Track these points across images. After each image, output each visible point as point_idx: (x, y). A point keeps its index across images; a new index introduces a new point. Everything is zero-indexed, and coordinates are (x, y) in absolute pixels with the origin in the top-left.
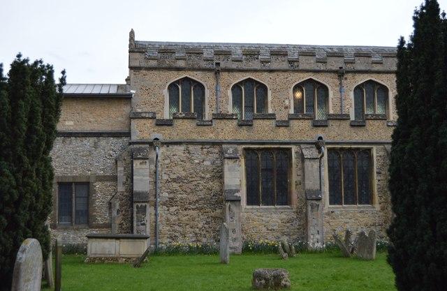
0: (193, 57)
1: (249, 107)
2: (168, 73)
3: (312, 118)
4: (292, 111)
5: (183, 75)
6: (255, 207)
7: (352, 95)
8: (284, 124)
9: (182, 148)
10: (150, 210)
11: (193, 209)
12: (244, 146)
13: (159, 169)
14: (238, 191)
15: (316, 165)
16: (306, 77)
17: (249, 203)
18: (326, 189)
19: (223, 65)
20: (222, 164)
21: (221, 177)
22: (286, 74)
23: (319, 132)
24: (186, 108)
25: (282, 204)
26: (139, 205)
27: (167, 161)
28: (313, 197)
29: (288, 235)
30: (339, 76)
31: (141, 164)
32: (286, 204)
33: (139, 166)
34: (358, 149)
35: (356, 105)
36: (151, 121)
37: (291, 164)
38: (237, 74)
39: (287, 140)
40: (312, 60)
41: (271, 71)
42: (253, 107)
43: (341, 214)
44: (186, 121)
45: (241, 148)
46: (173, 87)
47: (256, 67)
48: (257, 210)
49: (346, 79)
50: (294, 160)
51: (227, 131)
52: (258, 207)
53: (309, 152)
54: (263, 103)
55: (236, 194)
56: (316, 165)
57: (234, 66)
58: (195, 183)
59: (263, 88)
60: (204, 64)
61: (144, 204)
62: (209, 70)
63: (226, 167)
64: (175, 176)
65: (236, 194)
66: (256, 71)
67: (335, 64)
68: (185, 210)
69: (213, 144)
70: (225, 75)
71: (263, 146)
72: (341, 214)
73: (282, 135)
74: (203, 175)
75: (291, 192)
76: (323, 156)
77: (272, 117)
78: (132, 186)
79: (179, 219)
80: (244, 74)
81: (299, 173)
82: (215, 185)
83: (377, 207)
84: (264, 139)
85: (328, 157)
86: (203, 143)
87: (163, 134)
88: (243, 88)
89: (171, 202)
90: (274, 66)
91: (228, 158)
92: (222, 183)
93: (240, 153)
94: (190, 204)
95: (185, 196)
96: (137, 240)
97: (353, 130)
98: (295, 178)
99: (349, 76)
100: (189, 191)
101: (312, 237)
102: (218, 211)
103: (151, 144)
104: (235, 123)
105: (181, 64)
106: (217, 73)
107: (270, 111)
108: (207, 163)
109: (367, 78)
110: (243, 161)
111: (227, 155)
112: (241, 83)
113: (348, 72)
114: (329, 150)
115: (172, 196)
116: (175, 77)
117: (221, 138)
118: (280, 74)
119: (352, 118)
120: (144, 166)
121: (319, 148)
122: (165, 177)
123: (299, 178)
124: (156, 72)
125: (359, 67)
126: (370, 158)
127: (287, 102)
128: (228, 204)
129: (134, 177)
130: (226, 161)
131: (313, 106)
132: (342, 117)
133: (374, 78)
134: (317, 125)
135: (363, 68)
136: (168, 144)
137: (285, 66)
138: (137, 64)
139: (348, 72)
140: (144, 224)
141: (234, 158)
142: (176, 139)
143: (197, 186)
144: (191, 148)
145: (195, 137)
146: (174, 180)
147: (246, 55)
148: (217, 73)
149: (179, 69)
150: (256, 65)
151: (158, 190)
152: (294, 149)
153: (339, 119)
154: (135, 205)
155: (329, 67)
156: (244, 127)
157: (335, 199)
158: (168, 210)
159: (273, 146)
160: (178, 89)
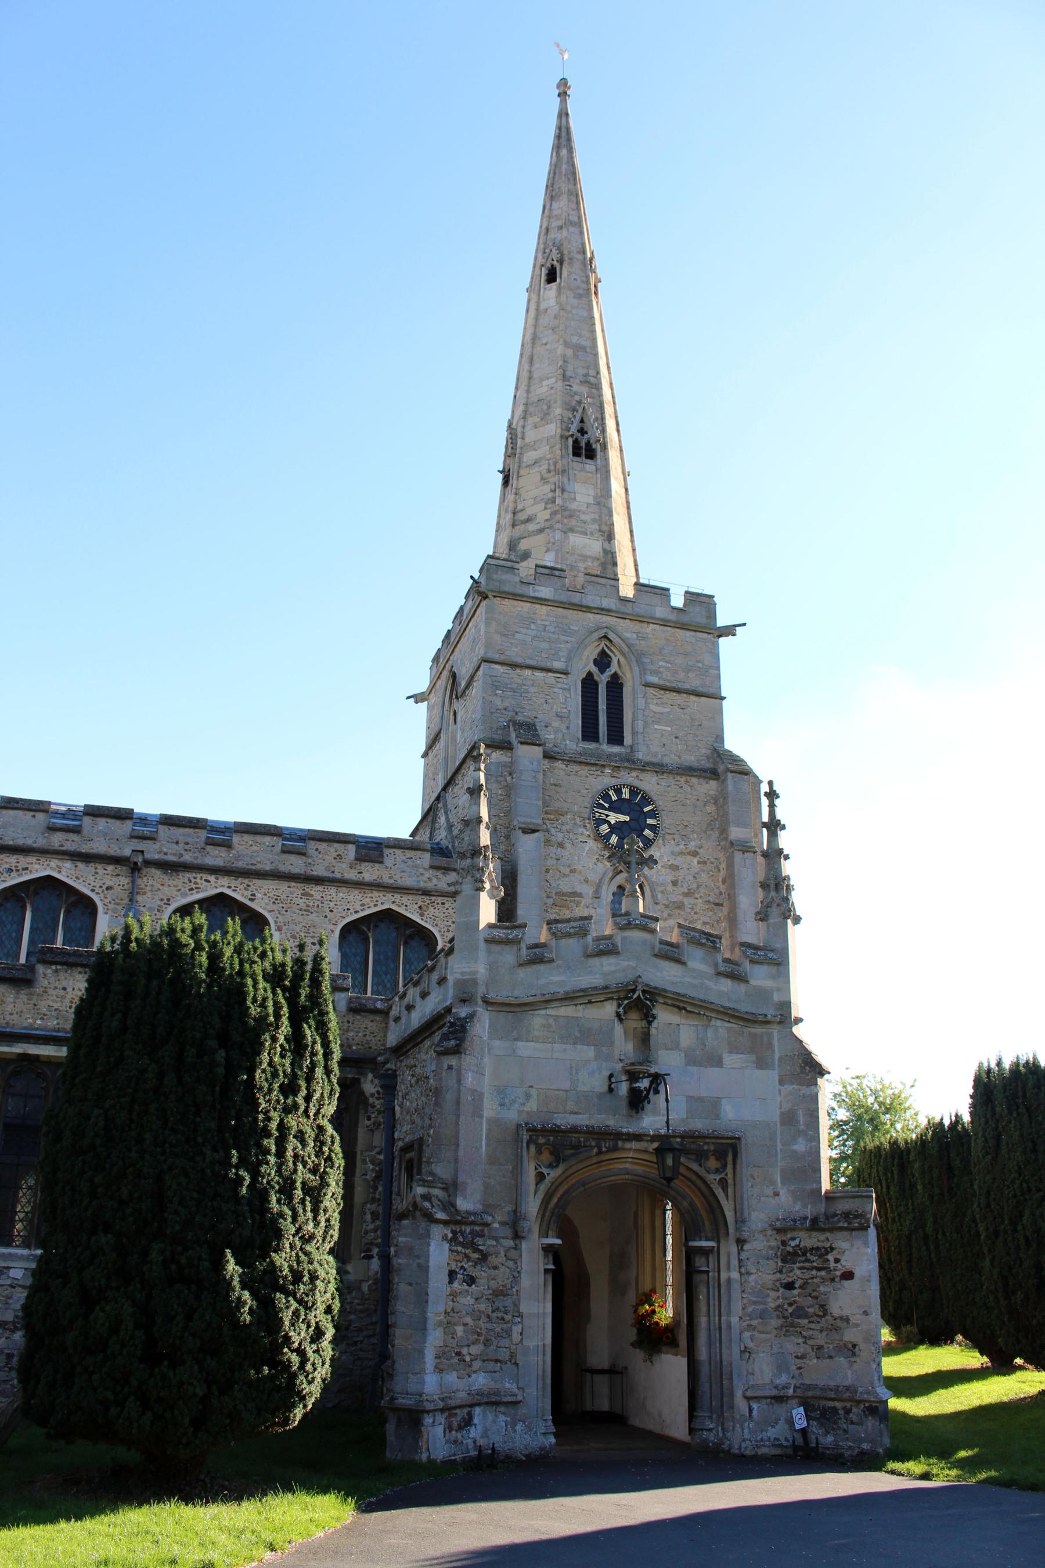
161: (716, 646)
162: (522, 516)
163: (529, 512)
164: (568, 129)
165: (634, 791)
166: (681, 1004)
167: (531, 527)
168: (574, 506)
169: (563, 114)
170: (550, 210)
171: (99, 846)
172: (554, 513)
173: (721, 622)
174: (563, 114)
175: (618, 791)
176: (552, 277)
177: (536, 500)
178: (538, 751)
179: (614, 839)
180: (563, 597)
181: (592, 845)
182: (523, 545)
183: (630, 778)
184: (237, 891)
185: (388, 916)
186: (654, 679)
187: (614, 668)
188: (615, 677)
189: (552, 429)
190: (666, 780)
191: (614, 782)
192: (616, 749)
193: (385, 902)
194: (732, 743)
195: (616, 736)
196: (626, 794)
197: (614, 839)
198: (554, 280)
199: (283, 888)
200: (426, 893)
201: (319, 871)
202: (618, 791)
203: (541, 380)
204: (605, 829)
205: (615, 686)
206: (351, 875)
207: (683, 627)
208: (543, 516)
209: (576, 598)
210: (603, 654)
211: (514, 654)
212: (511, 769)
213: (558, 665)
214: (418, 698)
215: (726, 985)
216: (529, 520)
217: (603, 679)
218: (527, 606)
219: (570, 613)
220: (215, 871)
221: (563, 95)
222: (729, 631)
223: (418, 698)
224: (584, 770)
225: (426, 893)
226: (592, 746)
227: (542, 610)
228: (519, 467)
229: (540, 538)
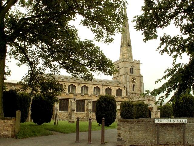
15: (74, 103)
16: (71, 84)
23: (75, 97)
28: (73, 110)
53: (73, 101)
73: (67, 97)
83: (86, 113)
84: (64, 98)
97: (82, 96)
109: (84, 85)
114: (77, 100)
121: (75, 100)
125: (82, 82)
126: (85, 102)
133: (86, 85)
137: (67, 81)
155: (76, 82)
157: (77, 111)
166: (151, 100)
171: (100, 84)
173: (140, 63)
182: (124, 54)
184: (109, 87)
185: (119, 89)
194: (141, 74)
195: (133, 73)
199: (113, 87)
205: (133, 68)
212: (126, 77)
220: (108, 86)
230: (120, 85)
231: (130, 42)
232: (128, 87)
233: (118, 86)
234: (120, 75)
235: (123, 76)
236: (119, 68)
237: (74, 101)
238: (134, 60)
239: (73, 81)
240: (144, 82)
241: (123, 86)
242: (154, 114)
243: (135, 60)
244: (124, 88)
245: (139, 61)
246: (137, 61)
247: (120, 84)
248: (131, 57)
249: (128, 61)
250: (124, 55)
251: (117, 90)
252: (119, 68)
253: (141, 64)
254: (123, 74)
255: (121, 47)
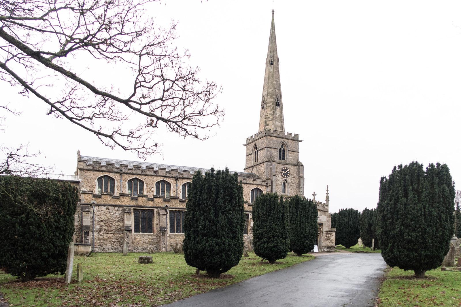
0: (110, 166)
1: (136, 190)
2: (97, 173)
3: (162, 197)
4: (155, 194)
5: (105, 174)
6: (138, 233)
7: (181, 187)
8: (152, 200)
9: (105, 207)
10: (91, 233)
11: (110, 234)
12: (134, 208)
13: (95, 216)
14: (131, 226)
15: (165, 217)
16: (162, 179)
17: (135, 231)
18: (168, 227)
19: (124, 171)
20: (124, 215)
21: (123, 220)
22: (153, 177)
24: (106, 189)
25: (150, 232)
26: (86, 231)
27: (98, 213)
29: (152, 245)
30: (176, 179)
31: (86, 213)
32: (152, 232)
33: (85, 215)
34: (182, 211)
35: (183, 192)
36: (91, 195)
37: (154, 216)
38: (130, 176)
39: (152, 206)
40: (164, 172)
41: (146, 175)
42: (137, 190)
43: (174, 237)
44: (107, 196)
45: (132, 208)
46: (100, 179)
47: (139, 173)
48: (139, 234)
49: (179, 181)
50: (155, 214)
51: (126, 201)
52: (139, 233)
53: (163, 212)
54: (142, 189)
55: (130, 228)
56: (165, 217)
57: (129, 172)
58: (111, 222)
59: (142, 182)
60: (115, 170)
61: (88, 231)
62: (118, 173)
63: (125, 216)
64: (102, 219)
65: (130, 228)
66: (139, 175)
67: (174, 174)
68: (107, 234)
69: (120, 206)
70: (125, 176)
71: (142, 208)
72: (174, 237)
73: (151, 204)
74: (115, 219)
75: (154, 228)
76: (167, 213)
77: (146, 196)
78: (82, 223)
79: (104, 238)
80: (133, 176)
81: (158, 220)
82: (121, 224)
85: (170, 214)
86: (115, 206)
87: (96, 201)
88: (133, 182)
89: (100, 230)
90: (148, 173)
91: (127, 213)
92: (124, 223)
93: (132, 210)
94: (109, 231)
95: (107, 228)
96: (86, 246)
98: (155, 221)
99: (180, 180)
100: (108, 226)
101: (162, 246)
102: (122, 235)
103: (91, 205)
104: (130, 198)
105: (104, 169)
106: (121, 174)
107: (145, 193)
108: (117, 214)
110: (133, 214)
111: (126, 211)
112: (132, 179)
113: (180, 178)
114: (170, 211)
115: (101, 227)
116: (101, 174)
117: (123, 204)
118: (150, 177)
119: (181, 198)
120: (87, 215)
121: (166, 211)
122: (98, 220)
123: (157, 222)
124: (92, 172)
127: (153, 189)
128: (126, 232)
129: (83, 219)
130: (126, 214)
131: (164, 191)
132: (176, 198)
134: (165, 201)
135: (186, 176)
136: (99, 205)
137: (152, 173)
138: (82, 167)
139: (180, 178)
140: (88, 239)
141: (130, 213)
142: (103, 203)
143: (112, 224)
144: (110, 207)
145: (112, 203)
146: (102, 221)
147: (135, 167)
148: (121, 174)
149: (103, 171)
150: (139, 172)
151: (94, 225)
152: (155, 210)
153: (175, 199)
154: (83, 232)
155: (172, 175)
156: (134, 200)
157: (172, 231)
158: (99, 234)
159: (146, 208)
160: (102, 180)
161: (298, 143)
162: (267, 117)
163: (269, 116)
164: (274, 24)
165: (287, 168)
167: (269, 119)
168: (276, 116)
169: (273, 20)
170: (271, 46)
172: (273, 118)
173: (299, 139)
174: (273, 20)
175: (284, 168)
176: (272, 64)
177: (270, 114)
178: (275, 163)
179: (284, 176)
180: (277, 136)
181: (281, 176)
182: (268, 123)
183: (286, 166)
185: (257, 188)
186: (290, 150)
187: (284, 148)
188: (284, 149)
189: (272, 100)
190: (291, 166)
191: (284, 167)
192: (284, 161)
193: (257, 186)
195: (284, 159)
196: (286, 169)
197: (284, 176)
198: (272, 65)
200: (262, 185)
201: (248, 182)
202: (284, 168)
203: (271, 88)
204: (283, 174)
205: (284, 150)
206: (252, 183)
207: (294, 140)
208: (271, 117)
209: (279, 136)
210: (282, 145)
211: (270, 146)
212: (271, 165)
213: (276, 147)
214: (244, 145)
215: (322, 208)
216: (269, 118)
217: (282, 149)
218: (272, 138)
219: (278, 138)
221: (273, 14)
222: (301, 141)
223: (244, 145)
224: (280, 165)
225: (262, 185)
226: (280, 160)
227: (274, 138)
228: (266, 107)
229: (271, 122)
230: (259, 182)
231: (281, 98)
232: (274, 184)
233: (255, 182)
234: (258, 163)
235: (265, 164)
236: (256, 149)
237: (164, 212)
238: (286, 134)
239: (165, 175)
240: (304, 176)
241: (263, 184)
242: (325, 236)
243: (289, 134)
244: (267, 187)
245: (296, 135)
246: (293, 136)
247: (258, 180)
248: (282, 127)
249: (275, 135)
250: (268, 125)
251: (253, 191)
252: (256, 149)
253: (301, 141)
254: (265, 160)
255: (263, 108)
